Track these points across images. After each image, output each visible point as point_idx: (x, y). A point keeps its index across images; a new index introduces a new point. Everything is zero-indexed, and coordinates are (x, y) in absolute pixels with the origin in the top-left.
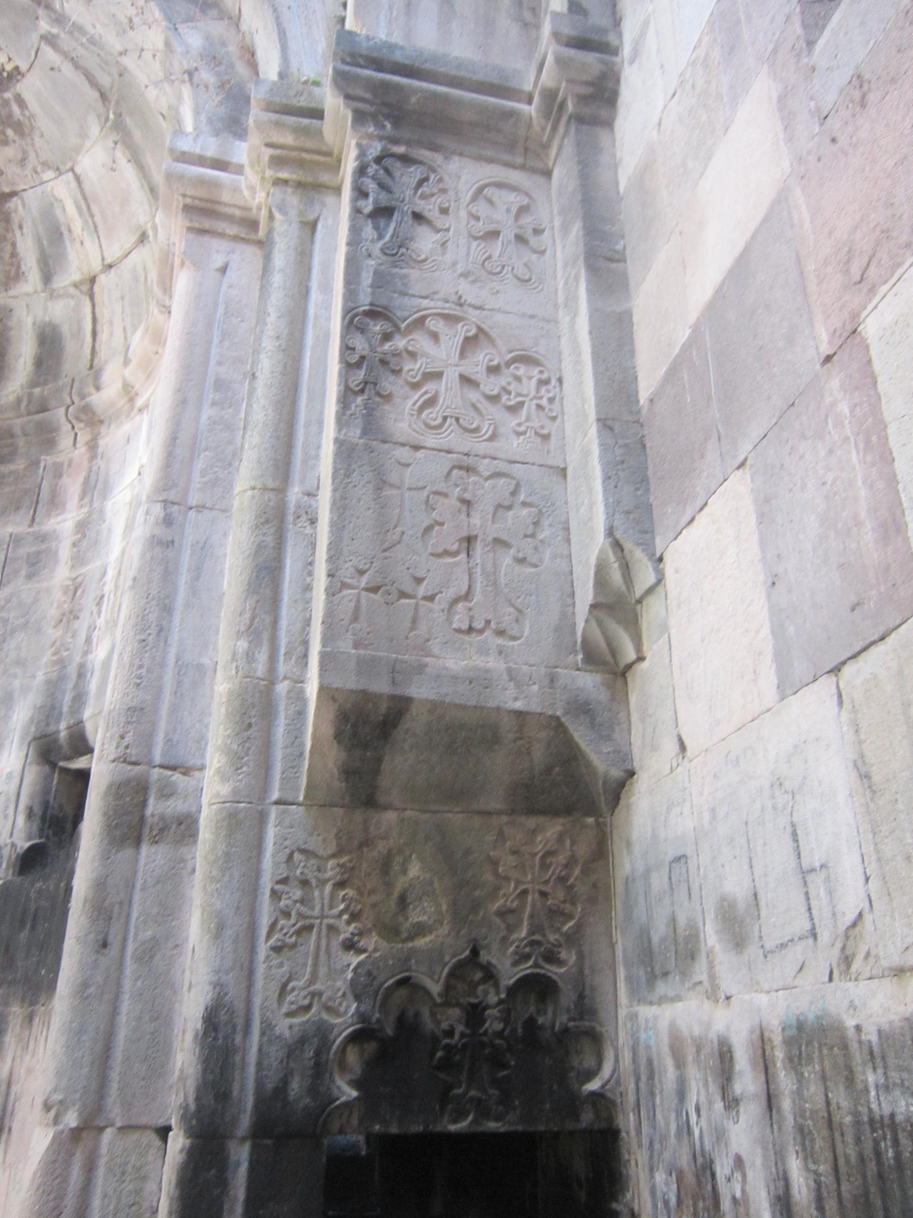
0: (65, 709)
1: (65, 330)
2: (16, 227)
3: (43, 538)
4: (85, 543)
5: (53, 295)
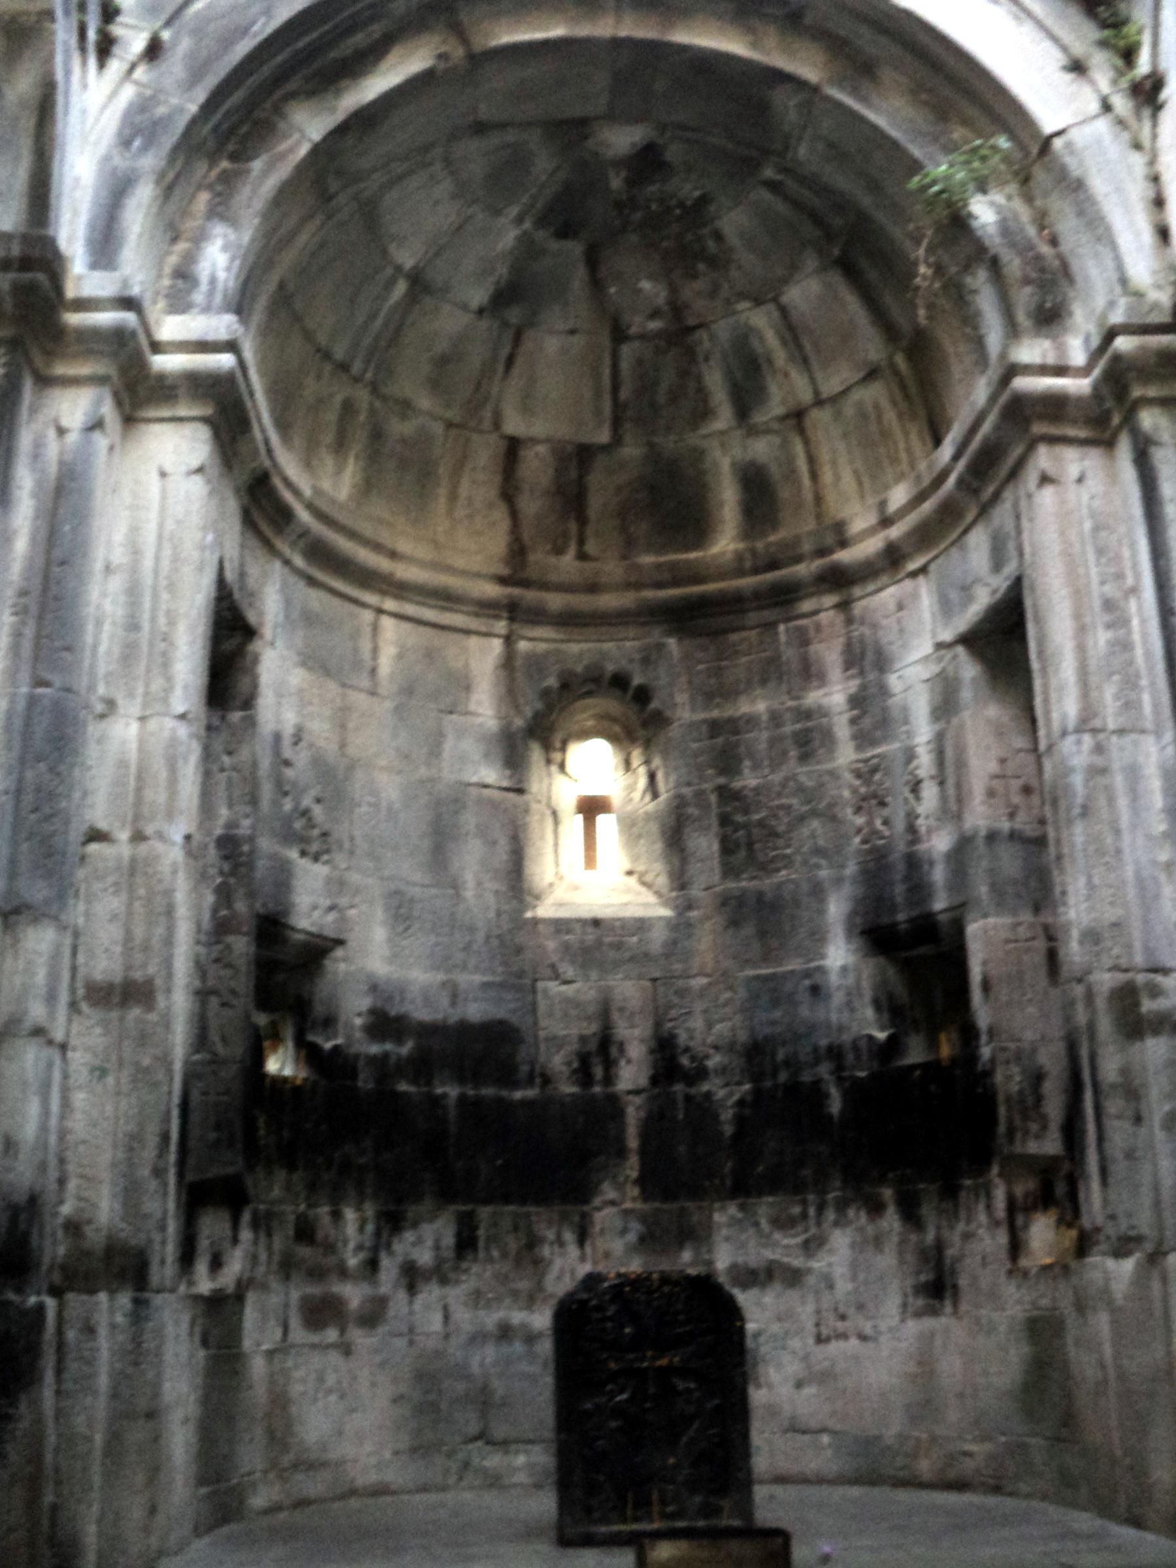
0: (899, 899)
1: (775, 471)
2: (701, 358)
3: (807, 714)
4: (867, 722)
5: (753, 432)
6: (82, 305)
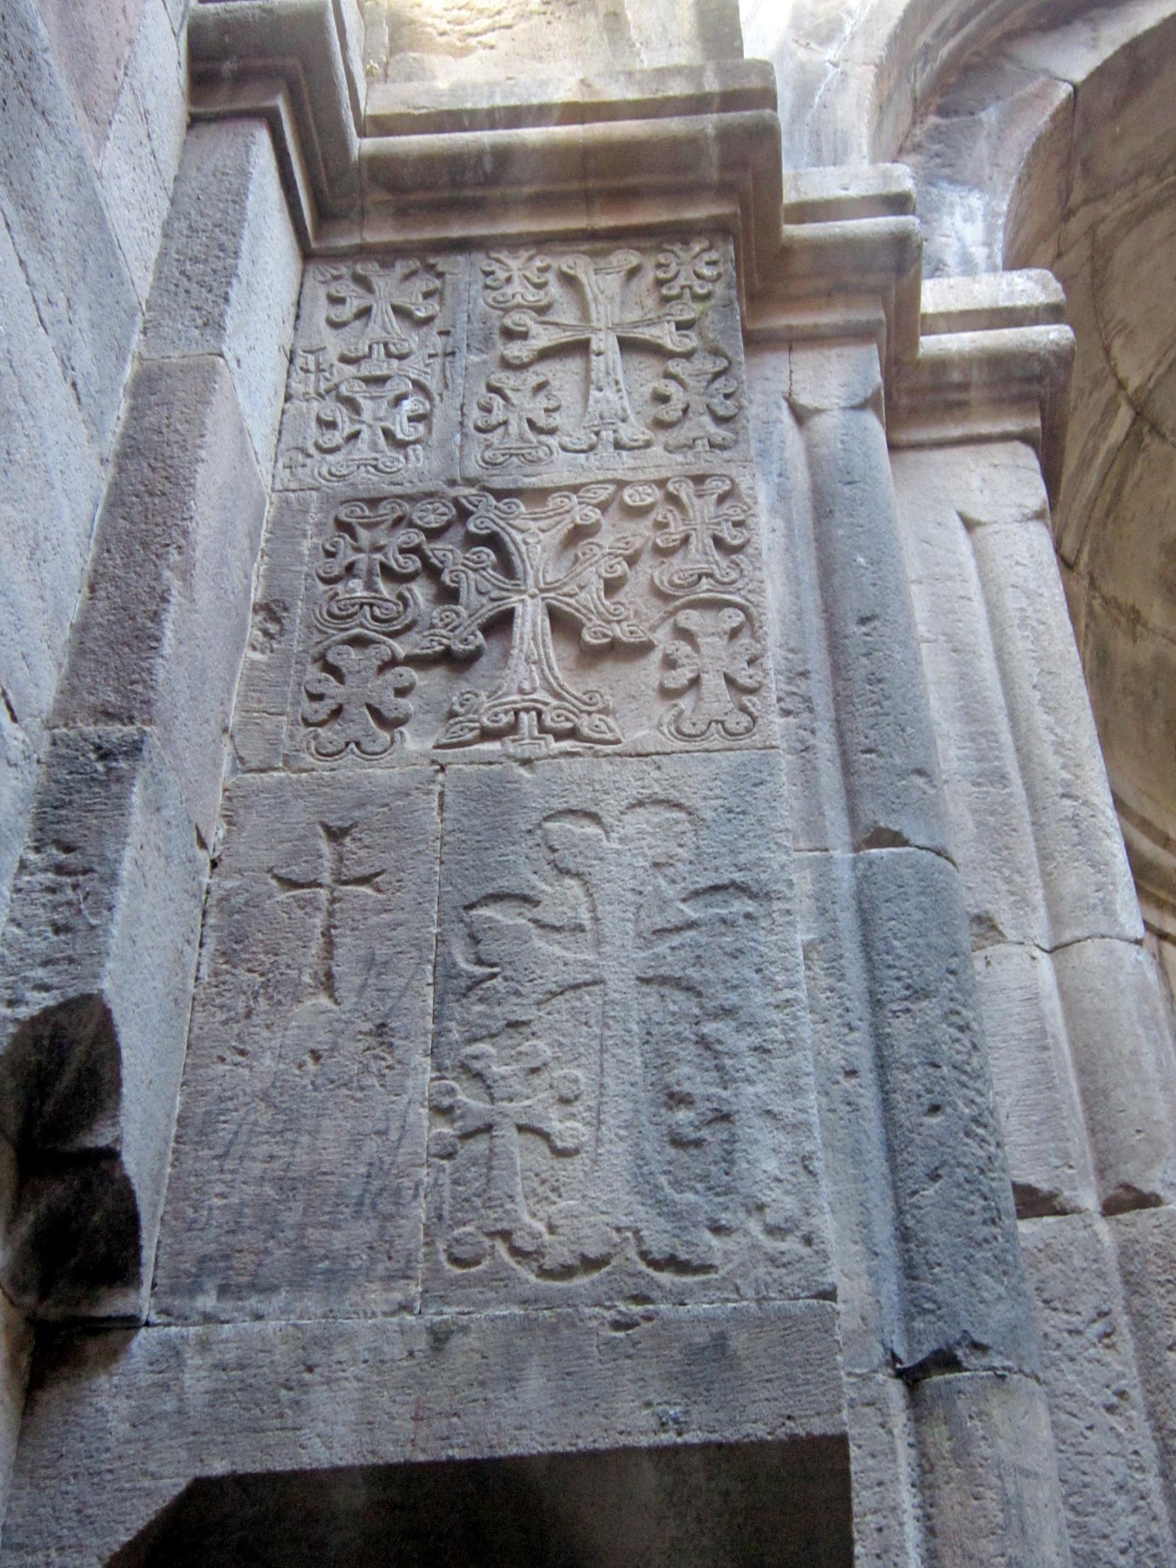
6: (808, 211)
